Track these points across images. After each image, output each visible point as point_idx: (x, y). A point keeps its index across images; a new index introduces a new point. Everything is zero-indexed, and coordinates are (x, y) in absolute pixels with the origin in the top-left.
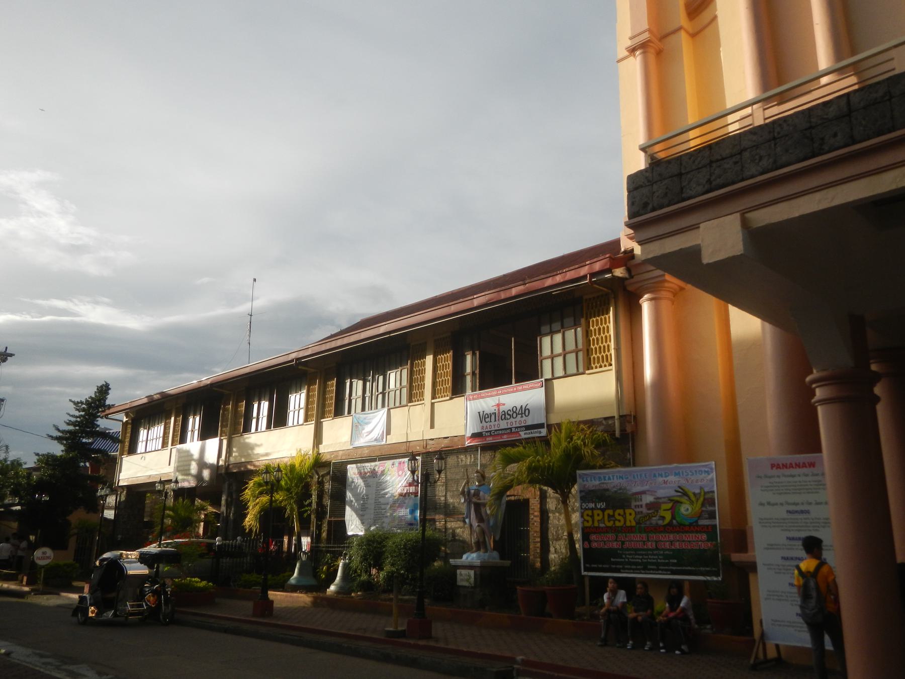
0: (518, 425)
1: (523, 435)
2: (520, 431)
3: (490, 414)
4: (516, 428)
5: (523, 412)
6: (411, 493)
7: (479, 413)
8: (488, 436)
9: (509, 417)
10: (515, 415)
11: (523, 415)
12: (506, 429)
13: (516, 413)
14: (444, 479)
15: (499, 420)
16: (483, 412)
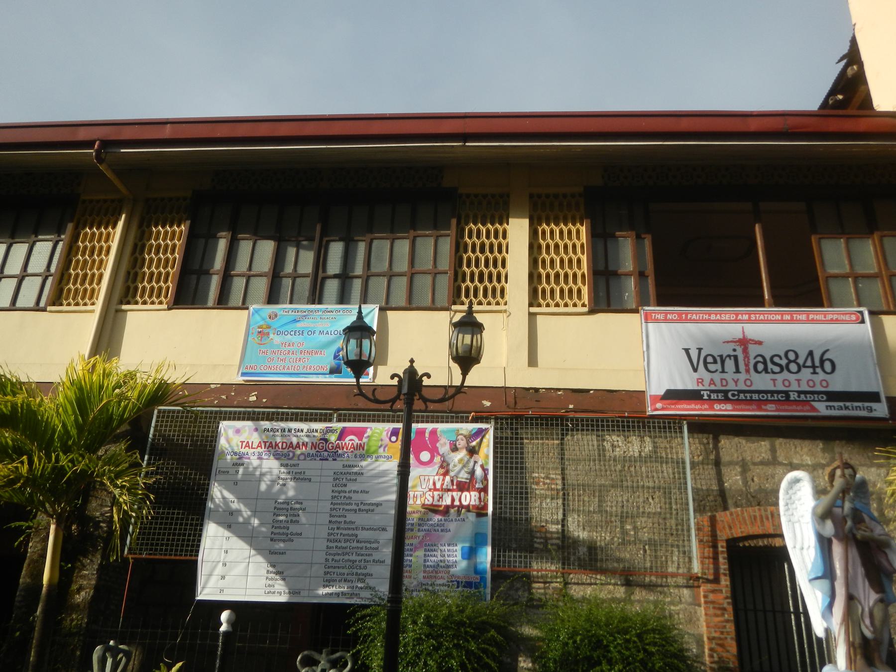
0: (805, 387)
1: (822, 408)
2: (814, 401)
3: (721, 356)
4: (800, 393)
5: (817, 363)
6: (468, 508)
7: (687, 351)
8: (719, 401)
9: (777, 369)
10: (794, 367)
11: (818, 370)
12: (772, 392)
13: (798, 364)
14: (559, 482)
15: (748, 371)
16: (700, 350)
